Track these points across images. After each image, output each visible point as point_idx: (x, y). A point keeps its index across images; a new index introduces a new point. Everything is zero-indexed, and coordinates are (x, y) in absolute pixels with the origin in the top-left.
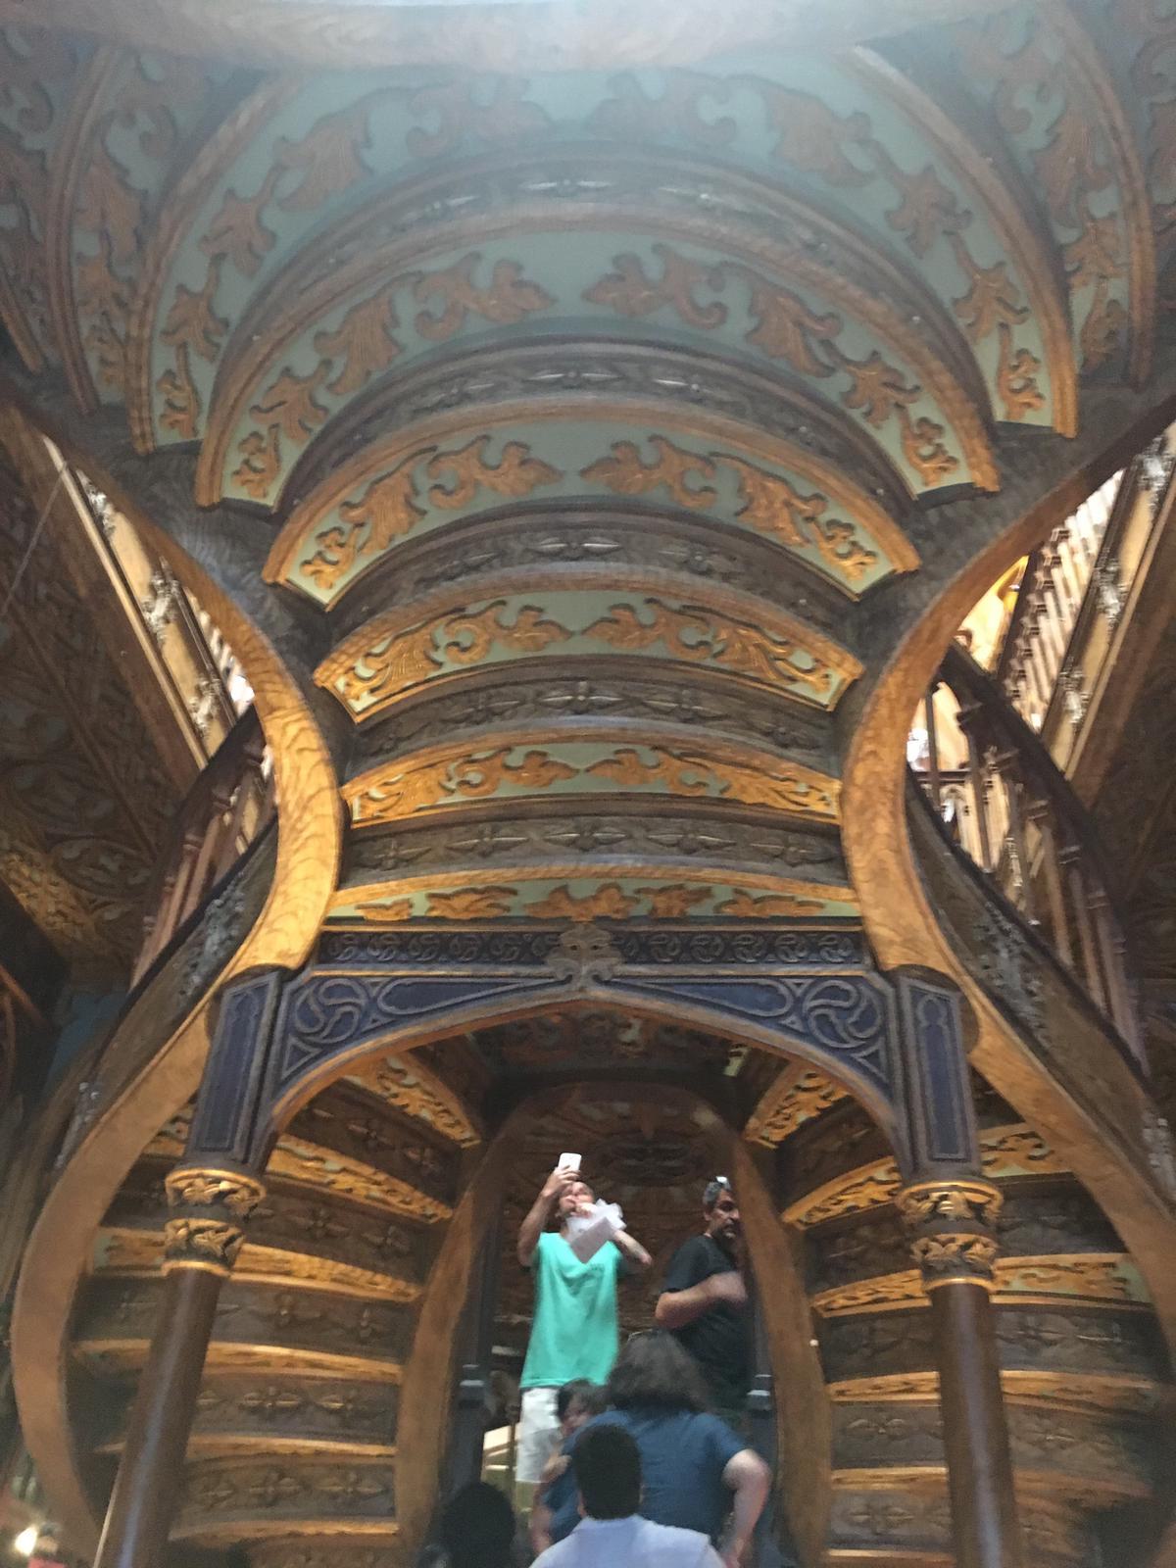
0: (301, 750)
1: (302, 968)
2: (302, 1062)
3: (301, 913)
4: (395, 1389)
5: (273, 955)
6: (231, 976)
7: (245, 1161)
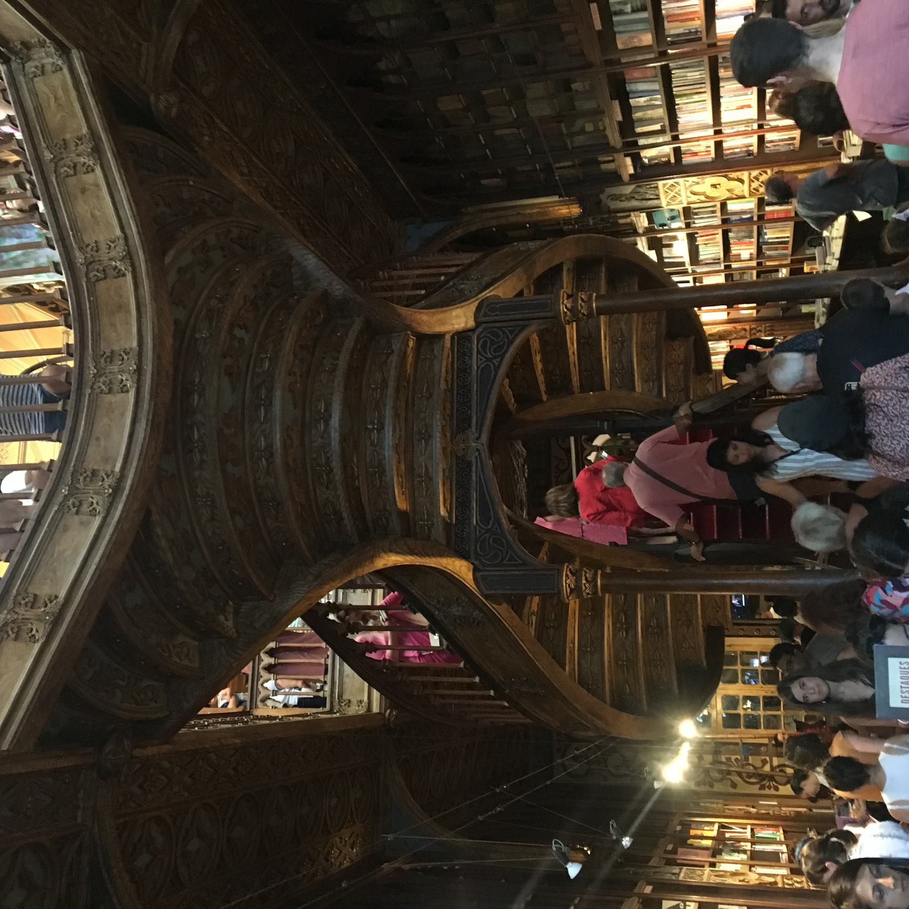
1: (472, 563)
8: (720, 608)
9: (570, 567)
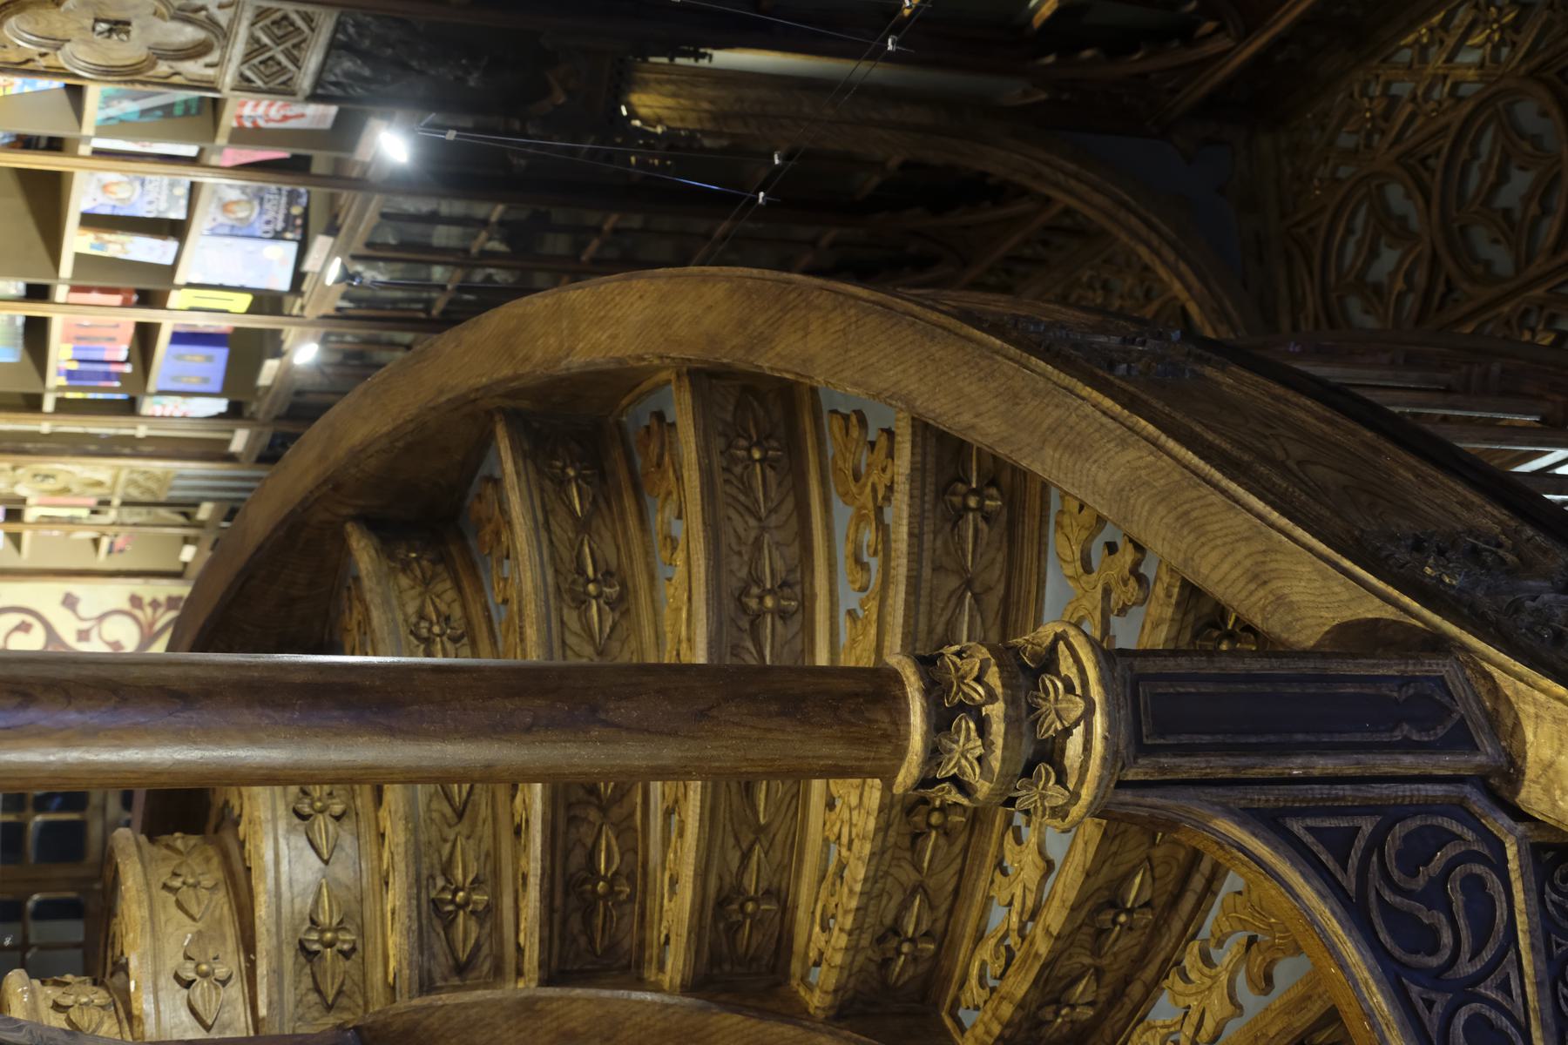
1: (1519, 815)
5: (1547, 753)
6: (1496, 673)
7: (1121, 785)
8: (165, 887)
9: (1057, 796)
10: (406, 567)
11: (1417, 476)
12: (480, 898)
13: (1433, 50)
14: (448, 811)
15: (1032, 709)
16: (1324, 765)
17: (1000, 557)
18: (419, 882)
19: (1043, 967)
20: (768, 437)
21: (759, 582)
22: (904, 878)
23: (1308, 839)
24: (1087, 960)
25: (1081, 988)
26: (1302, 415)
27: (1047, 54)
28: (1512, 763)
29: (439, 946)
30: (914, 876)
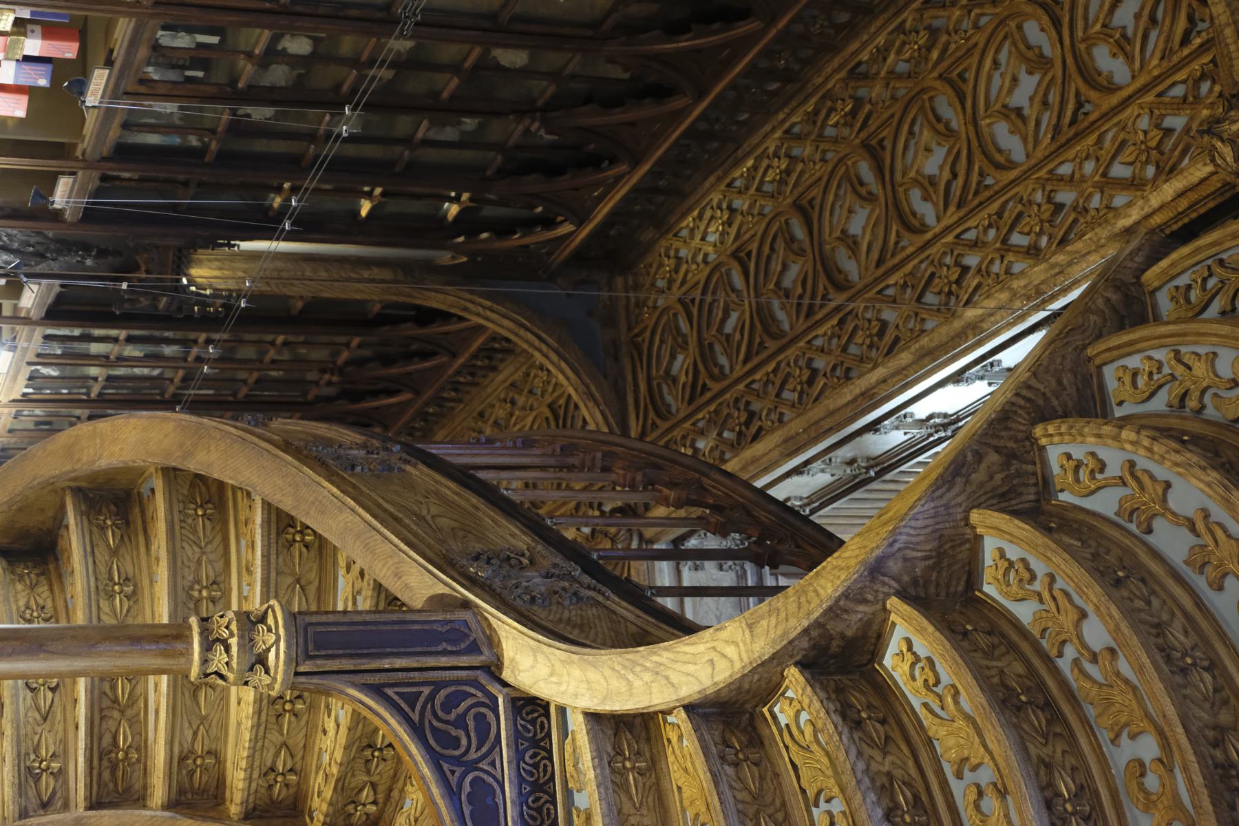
0: (711, 661)
1: (505, 684)
2: (403, 705)
3: (554, 679)
4: (137, 799)
7: (297, 674)
9: (267, 680)
10: (21, 578)
11: (493, 521)
12: (55, 765)
13: (696, 231)
14: (38, 717)
15: (251, 640)
16: (400, 663)
17: (315, 566)
18: (19, 757)
19: (338, 781)
20: (209, 502)
21: (199, 582)
22: (274, 739)
23: (395, 697)
24: (366, 779)
25: (365, 793)
26: (447, 491)
27: (459, 236)
28: (499, 659)
29: (32, 793)
30: (280, 739)
